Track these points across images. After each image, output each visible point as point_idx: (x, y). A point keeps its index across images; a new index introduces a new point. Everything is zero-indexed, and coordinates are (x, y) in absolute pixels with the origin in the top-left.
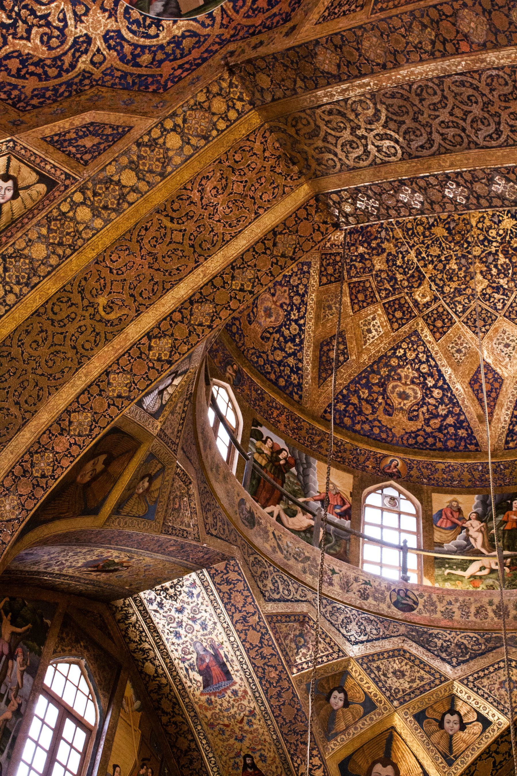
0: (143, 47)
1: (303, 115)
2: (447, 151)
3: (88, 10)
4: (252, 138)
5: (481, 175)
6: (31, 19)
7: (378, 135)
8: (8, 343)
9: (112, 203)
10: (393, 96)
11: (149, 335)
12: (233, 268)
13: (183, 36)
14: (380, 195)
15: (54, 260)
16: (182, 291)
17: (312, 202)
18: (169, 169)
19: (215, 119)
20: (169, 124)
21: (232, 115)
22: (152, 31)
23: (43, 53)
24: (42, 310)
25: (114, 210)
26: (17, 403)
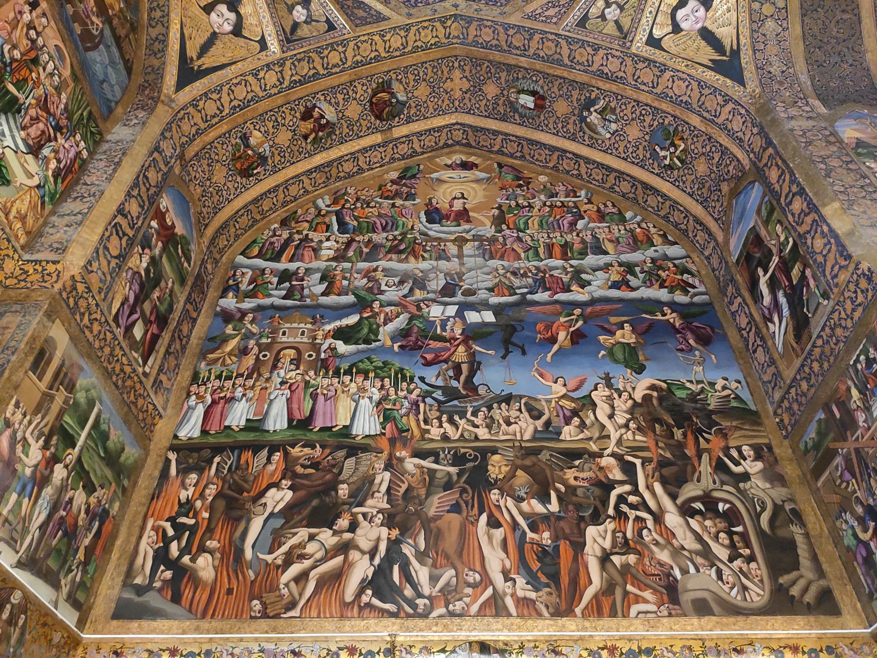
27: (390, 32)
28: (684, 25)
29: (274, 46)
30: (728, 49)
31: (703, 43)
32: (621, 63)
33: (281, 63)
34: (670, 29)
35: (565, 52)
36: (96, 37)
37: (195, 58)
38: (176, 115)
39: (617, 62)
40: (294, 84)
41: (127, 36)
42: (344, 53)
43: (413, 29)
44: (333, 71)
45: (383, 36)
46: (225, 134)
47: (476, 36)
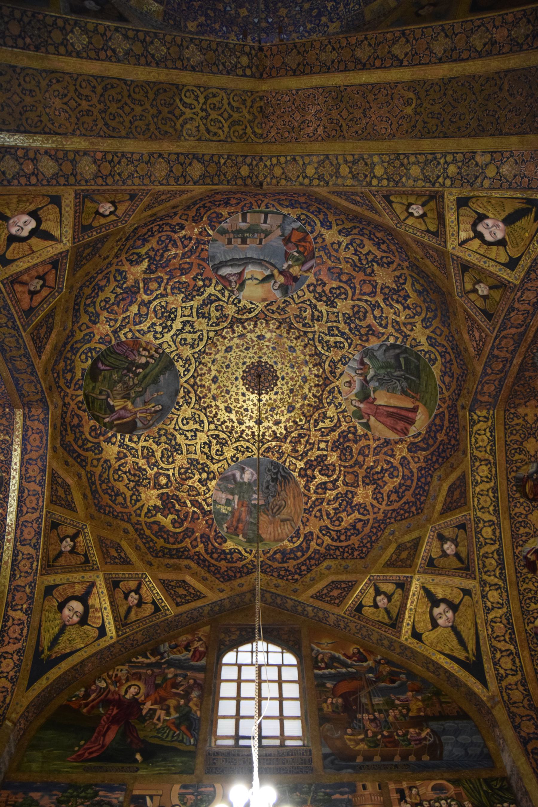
0: (312, 213)
1: (234, 139)
2: (148, 83)
3: (332, 244)
4: (273, 140)
5: (133, 60)
6: (363, 258)
7: (192, 109)
8: (473, 133)
9: (361, 164)
10: (166, 132)
11: (401, 65)
12: (329, 69)
13: (287, 207)
14: (215, 63)
15: (412, 159)
16: (364, 77)
17: (265, 76)
18: (322, 157)
19: (284, 166)
20: (307, 181)
21: (274, 161)
22: (303, 217)
23: (366, 242)
24: (441, 135)
25: (363, 159)
26: (501, 89)
27: (474, 476)
28: (500, 235)
29: (469, 584)
30: (524, 206)
31: (518, 223)
32: (529, 290)
33: (483, 583)
34: (501, 248)
35: (513, 331)
36: (434, 741)
37: (466, 655)
38: (504, 701)
39: (527, 293)
40: (503, 577)
41: (441, 703)
42: (485, 522)
43: (476, 453)
44: (498, 534)
45: (477, 483)
46: (531, 655)
47: (489, 396)
